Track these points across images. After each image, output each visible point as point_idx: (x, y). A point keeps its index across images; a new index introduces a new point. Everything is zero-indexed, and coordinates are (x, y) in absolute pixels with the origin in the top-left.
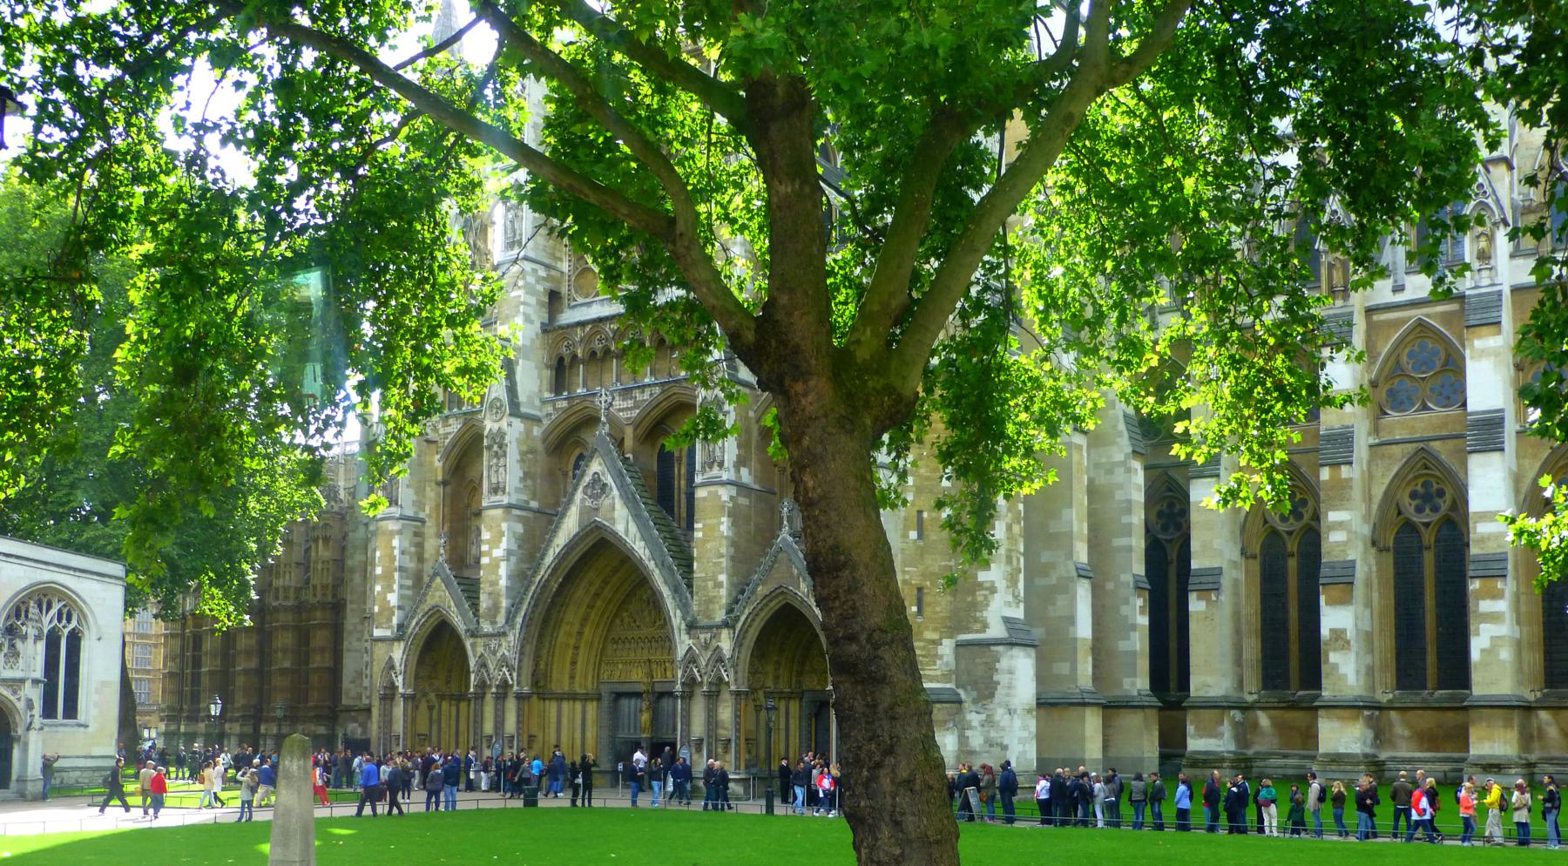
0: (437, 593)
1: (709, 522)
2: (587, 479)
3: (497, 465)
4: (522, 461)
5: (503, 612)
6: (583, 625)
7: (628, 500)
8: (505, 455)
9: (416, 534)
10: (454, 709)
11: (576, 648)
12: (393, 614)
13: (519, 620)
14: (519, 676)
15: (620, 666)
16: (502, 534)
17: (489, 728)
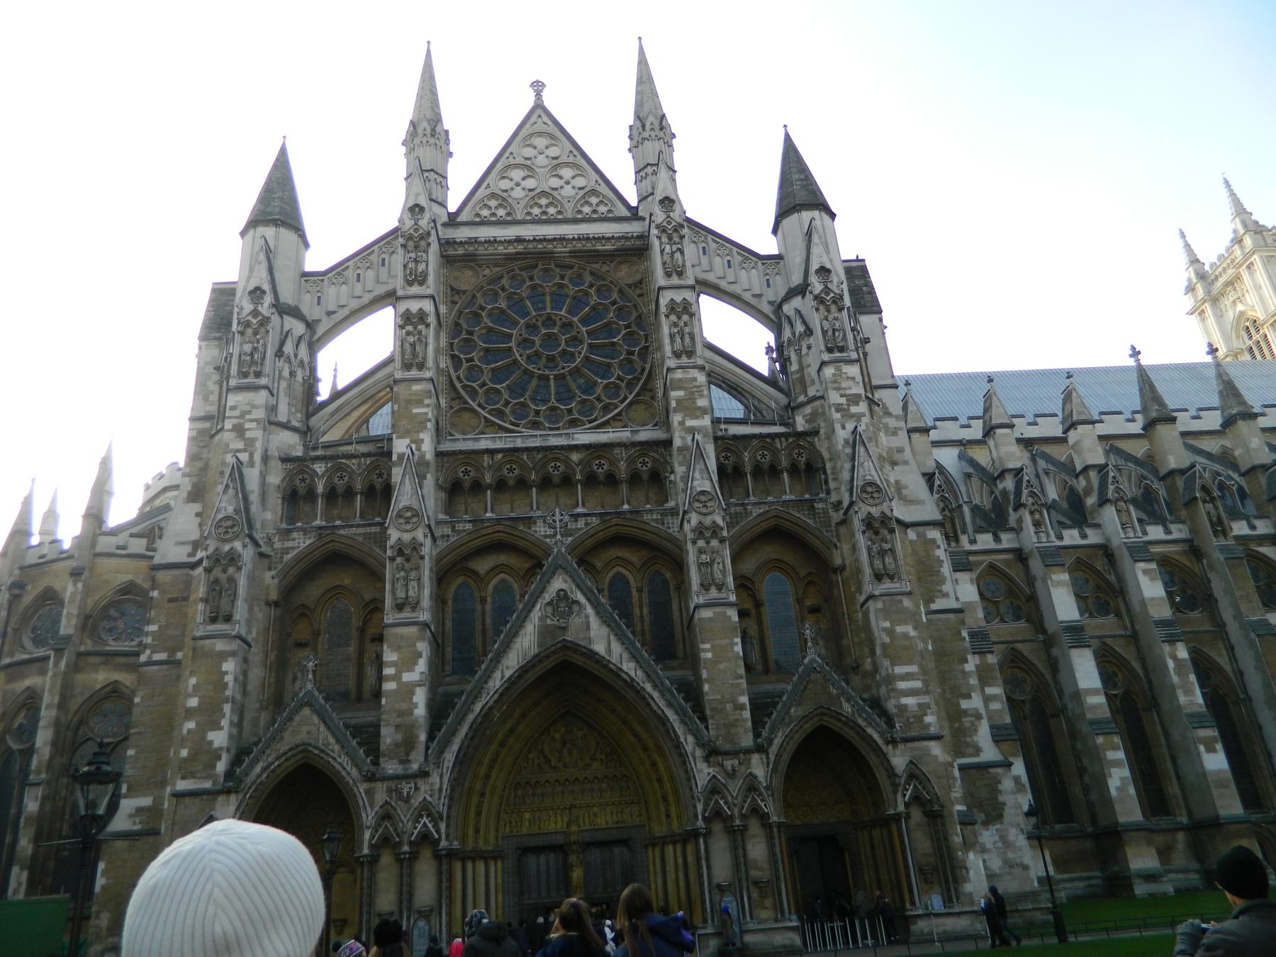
0: (304, 729)
1: (718, 642)
2: (548, 596)
3: (406, 578)
4: (431, 578)
5: (421, 748)
6: (491, 767)
7: (607, 621)
8: (417, 568)
9: (245, 660)
11: (483, 795)
12: (219, 758)
13: (449, 757)
14: (448, 827)
15: (527, 816)
16: (420, 655)
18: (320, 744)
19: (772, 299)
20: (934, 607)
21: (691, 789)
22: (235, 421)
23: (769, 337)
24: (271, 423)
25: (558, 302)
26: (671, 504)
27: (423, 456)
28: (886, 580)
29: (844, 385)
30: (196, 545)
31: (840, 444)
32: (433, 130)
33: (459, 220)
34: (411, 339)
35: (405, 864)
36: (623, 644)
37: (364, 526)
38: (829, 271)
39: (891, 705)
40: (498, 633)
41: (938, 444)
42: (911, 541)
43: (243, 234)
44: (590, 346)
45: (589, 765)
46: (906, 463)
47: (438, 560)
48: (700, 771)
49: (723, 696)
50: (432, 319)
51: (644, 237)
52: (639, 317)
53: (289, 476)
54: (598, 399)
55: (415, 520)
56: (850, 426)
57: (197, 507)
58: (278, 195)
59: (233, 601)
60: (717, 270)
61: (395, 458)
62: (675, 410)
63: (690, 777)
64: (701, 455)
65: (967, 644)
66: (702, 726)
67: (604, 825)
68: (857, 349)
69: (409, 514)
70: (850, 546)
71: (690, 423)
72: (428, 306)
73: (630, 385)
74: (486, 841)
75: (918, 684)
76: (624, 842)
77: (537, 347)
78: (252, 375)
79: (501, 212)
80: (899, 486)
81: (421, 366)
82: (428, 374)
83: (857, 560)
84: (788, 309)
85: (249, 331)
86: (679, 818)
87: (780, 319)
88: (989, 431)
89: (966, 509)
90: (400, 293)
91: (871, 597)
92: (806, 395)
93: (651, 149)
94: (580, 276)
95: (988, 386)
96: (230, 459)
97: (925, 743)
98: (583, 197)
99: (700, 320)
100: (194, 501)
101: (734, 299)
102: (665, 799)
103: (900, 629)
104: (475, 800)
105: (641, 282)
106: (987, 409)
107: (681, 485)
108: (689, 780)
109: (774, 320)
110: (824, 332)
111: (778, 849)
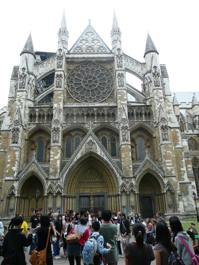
0: (33, 168)
1: (126, 153)
3: (55, 136)
5: (59, 173)
9: (20, 152)
10: (24, 201)
13: (65, 176)
14: (64, 190)
15: (81, 189)
16: (58, 153)
17: (50, 205)
18: (36, 171)
19: (143, 73)
20: (176, 147)
21: (118, 185)
22: (19, 98)
23: (141, 82)
24: (26, 99)
26: (117, 121)
27: (60, 108)
28: (165, 140)
29: (158, 94)
30: (10, 126)
32: (65, 31)
33: (70, 53)
34: (58, 81)
35: (54, 198)
36: (104, 152)
37: (46, 123)
38: (156, 67)
39: (164, 169)
40: (76, 149)
41: (180, 108)
42: (172, 132)
43: (21, 55)
44: (100, 83)
45: (95, 179)
46: (172, 113)
47: (63, 132)
48: (120, 182)
49: (126, 165)
50: (63, 76)
51: (113, 58)
52: (111, 77)
53: (30, 112)
54: (101, 96)
55: (58, 123)
56: (159, 104)
57: (10, 118)
58: (29, 46)
59: (18, 139)
60: (130, 66)
61: (54, 108)
62: (119, 99)
63: (118, 183)
64: (124, 110)
65: (183, 156)
66: (121, 172)
67: (98, 192)
68: (162, 86)
69: (57, 121)
70: (158, 132)
71: (122, 102)
72: (62, 73)
73: (109, 93)
74: (72, 194)
75: (171, 164)
76: (103, 196)
77: (87, 83)
78: (22, 88)
79: (80, 51)
80: (170, 119)
81: (60, 87)
82: (62, 89)
83: (159, 136)
84: (146, 76)
85: (22, 78)
86: (115, 191)
87: (144, 79)
88: (193, 106)
89: (186, 124)
90: (56, 70)
91: (162, 144)
92: (150, 97)
93: (116, 37)
94: (98, 66)
95: (194, 95)
96: (17, 107)
97: (172, 178)
98: (99, 48)
99: (125, 78)
100: (9, 116)
101: (134, 73)
102: (112, 187)
104: (70, 185)
105: (112, 68)
106: (193, 101)
107: (119, 117)
108: (118, 183)
109: (143, 78)
110: (155, 82)
111: (137, 199)
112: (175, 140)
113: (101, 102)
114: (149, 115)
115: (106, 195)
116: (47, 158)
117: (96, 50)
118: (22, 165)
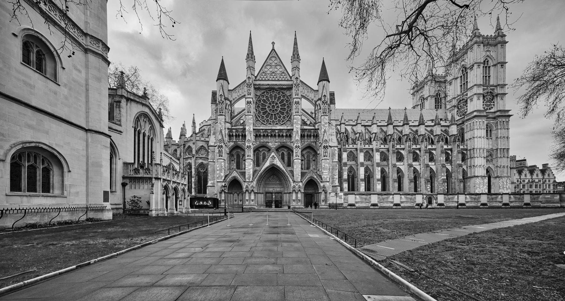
13: (256, 180)
17: (247, 198)
25: (275, 99)
31: (322, 132)
39: (323, 177)
40: (263, 161)
52: (290, 103)
60: (306, 92)
65: (337, 167)
71: (297, 126)
73: (287, 117)
75: (327, 174)
76: (281, 193)
84: (317, 103)
101: (308, 99)
103: (326, 165)
109: (315, 105)
112: (333, 155)
113: (281, 125)
114: (317, 136)
115: (283, 192)
116: (243, 167)
117: (278, 76)
118: (227, 172)
